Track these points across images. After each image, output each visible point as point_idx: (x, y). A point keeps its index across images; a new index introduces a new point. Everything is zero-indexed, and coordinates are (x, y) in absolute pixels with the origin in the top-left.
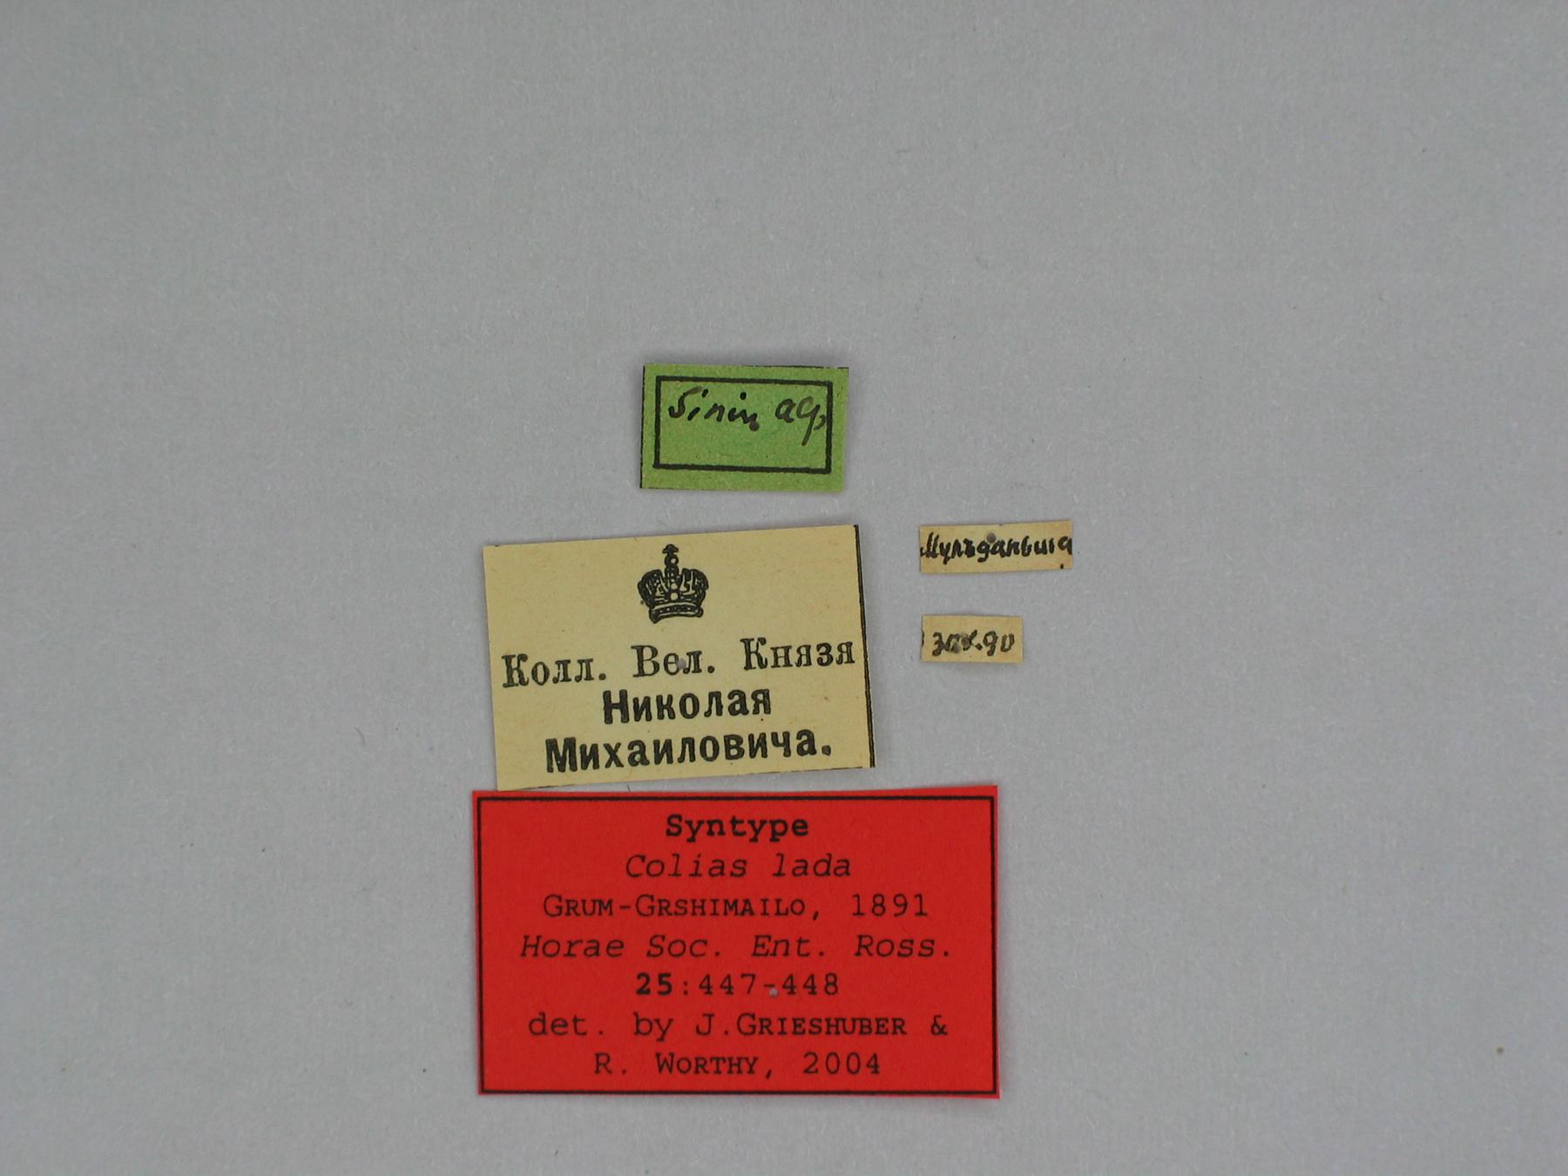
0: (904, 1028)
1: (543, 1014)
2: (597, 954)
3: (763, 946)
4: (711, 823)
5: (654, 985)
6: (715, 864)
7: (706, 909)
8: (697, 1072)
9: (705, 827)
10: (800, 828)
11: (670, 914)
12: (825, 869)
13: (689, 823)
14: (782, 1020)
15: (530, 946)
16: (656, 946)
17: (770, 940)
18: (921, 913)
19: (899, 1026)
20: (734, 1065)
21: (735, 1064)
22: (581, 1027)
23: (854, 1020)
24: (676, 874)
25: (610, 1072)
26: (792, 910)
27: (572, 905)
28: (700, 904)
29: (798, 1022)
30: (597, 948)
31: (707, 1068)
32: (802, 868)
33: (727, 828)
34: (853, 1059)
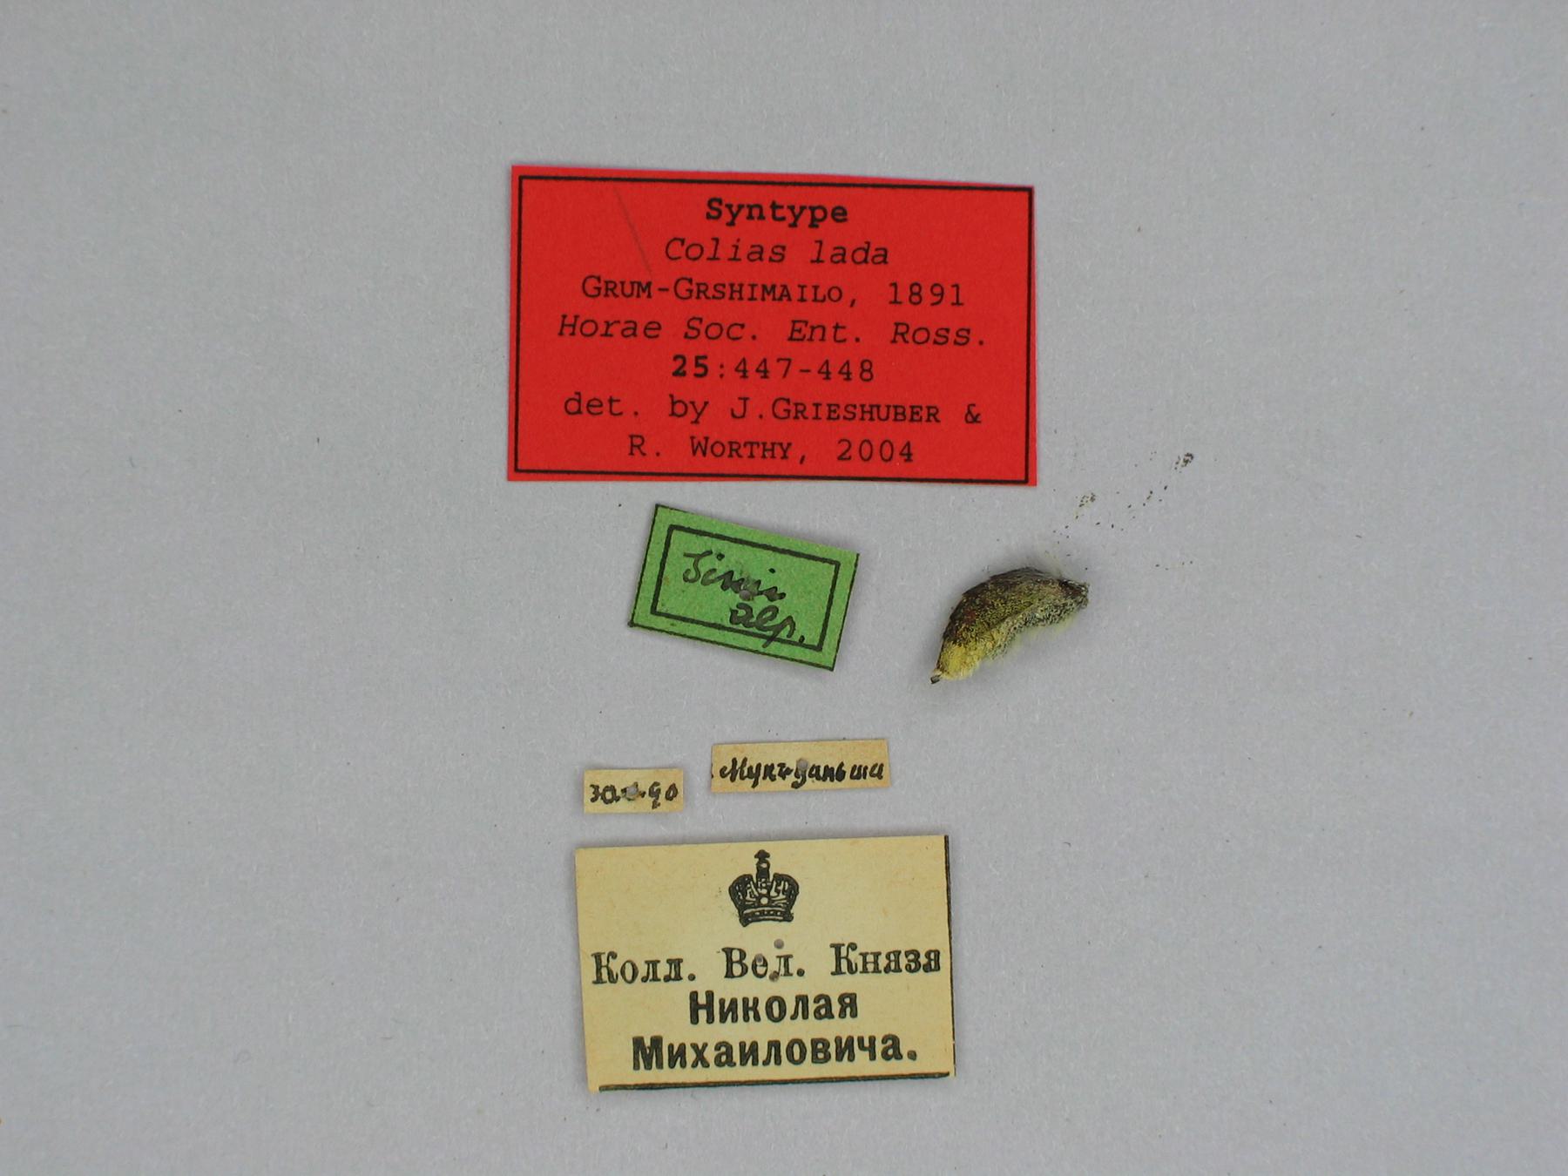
1: (579, 394)
2: (634, 334)
3: (800, 331)
4: (750, 208)
5: (690, 368)
6: (754, 249)
7: (743, 296)
8: (731, 456)
9: (745, 212)
10: (840, 214)
11: (707, 298)
12: (864, 256)
13: (729, 207)
14: (817, 405)
15: (566, 325)
16: (693, 328)
17: (806, 325)
18: (957, 303)
20: (768, 449)
21: (769, 450)
23: (888, 407)
24: (714, 258)
25: (644, 454)
26: (829, 297)
27: (611, 286)
28: (738, 289)
29: (833, 408)
30: (635, 329)
31: (741, 452)
32: (840, 256)
33: (768, 212)
34: (887, 447)
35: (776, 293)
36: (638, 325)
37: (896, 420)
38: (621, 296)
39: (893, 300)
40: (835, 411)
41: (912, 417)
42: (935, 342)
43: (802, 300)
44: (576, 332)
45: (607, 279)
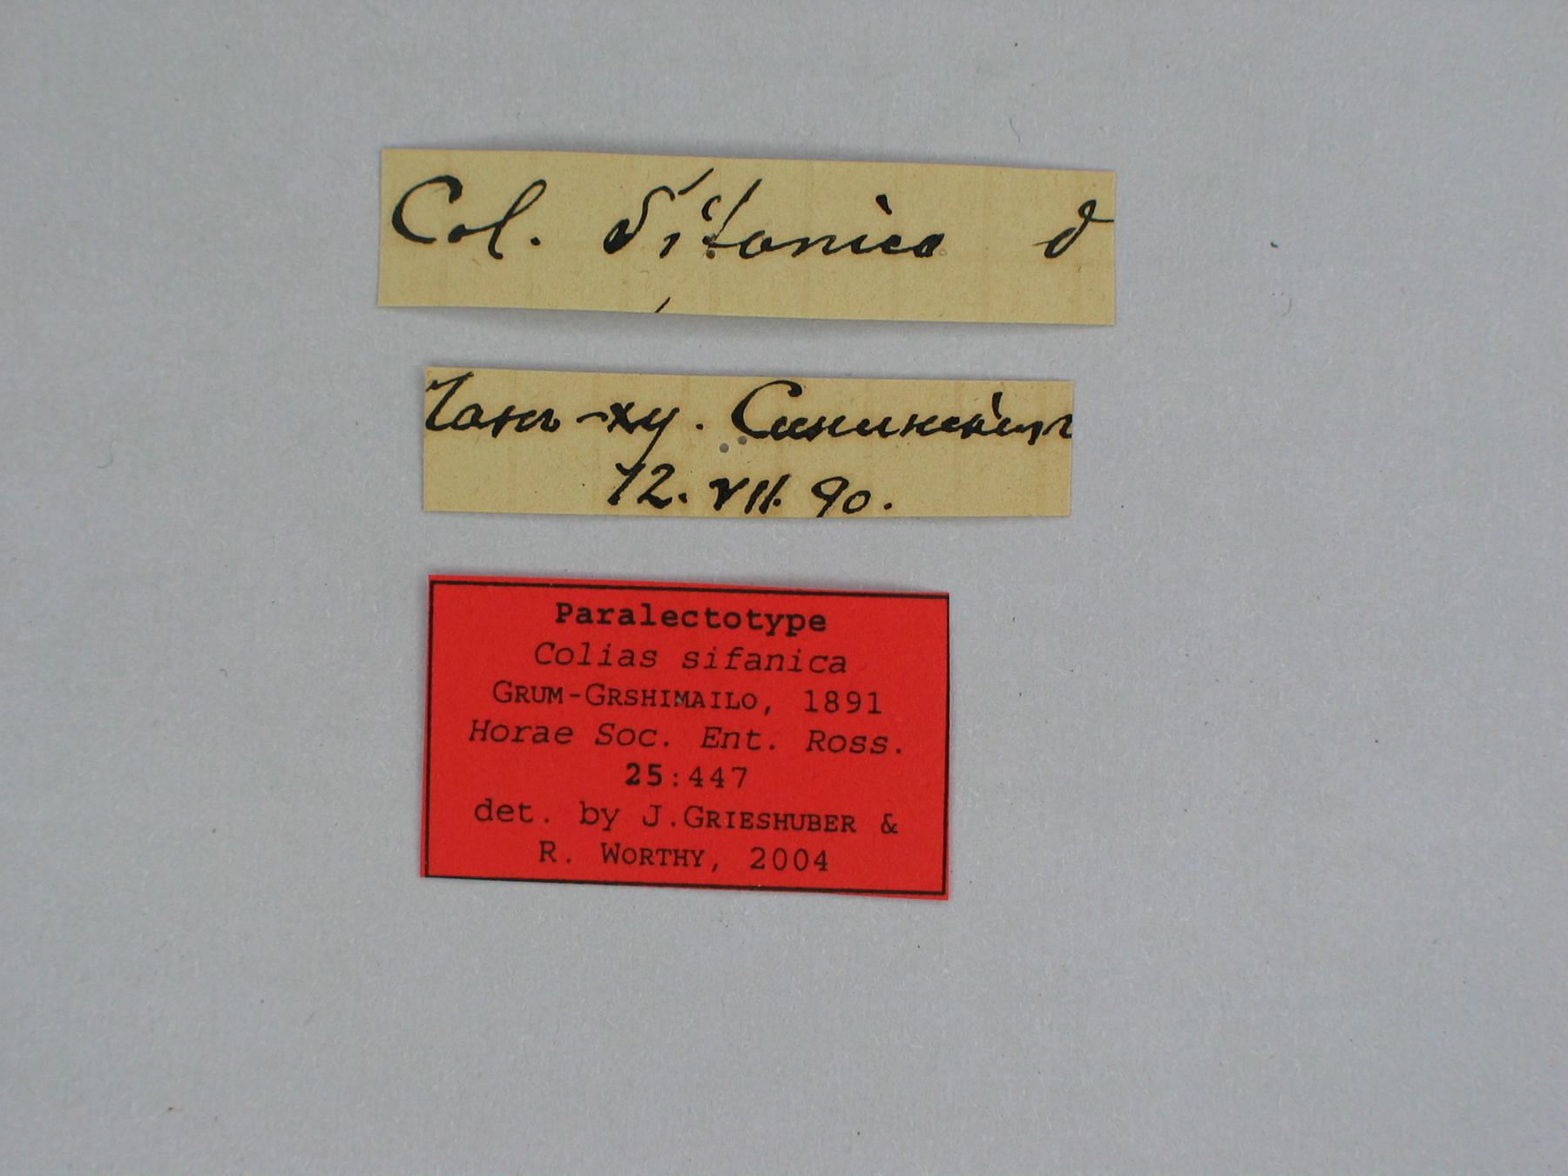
0: (853, 826)
2: (546, 740)
3: (713, 737)
7: (656, 701)
8: (642, 863)
11: (620, 704)
14: (731, 814)
15: (478, 730)
17: (720, 732)
18: (874, 711)
19: (848, 824)
20: (680, 857)
22: (526, 817)
23: (803, 816)
25: (554, 860)
29: (746, 817)
30: (546, 735)
35: (690, 698)
36: (550, 730)
37: (810, 829)
38: (532, 701)
39: (808, 707)
40: (748, 820)
41: (827, 826)
42: (851, 750)
43: (716, 706)
44: (487, 736)
45: (518, 684)
